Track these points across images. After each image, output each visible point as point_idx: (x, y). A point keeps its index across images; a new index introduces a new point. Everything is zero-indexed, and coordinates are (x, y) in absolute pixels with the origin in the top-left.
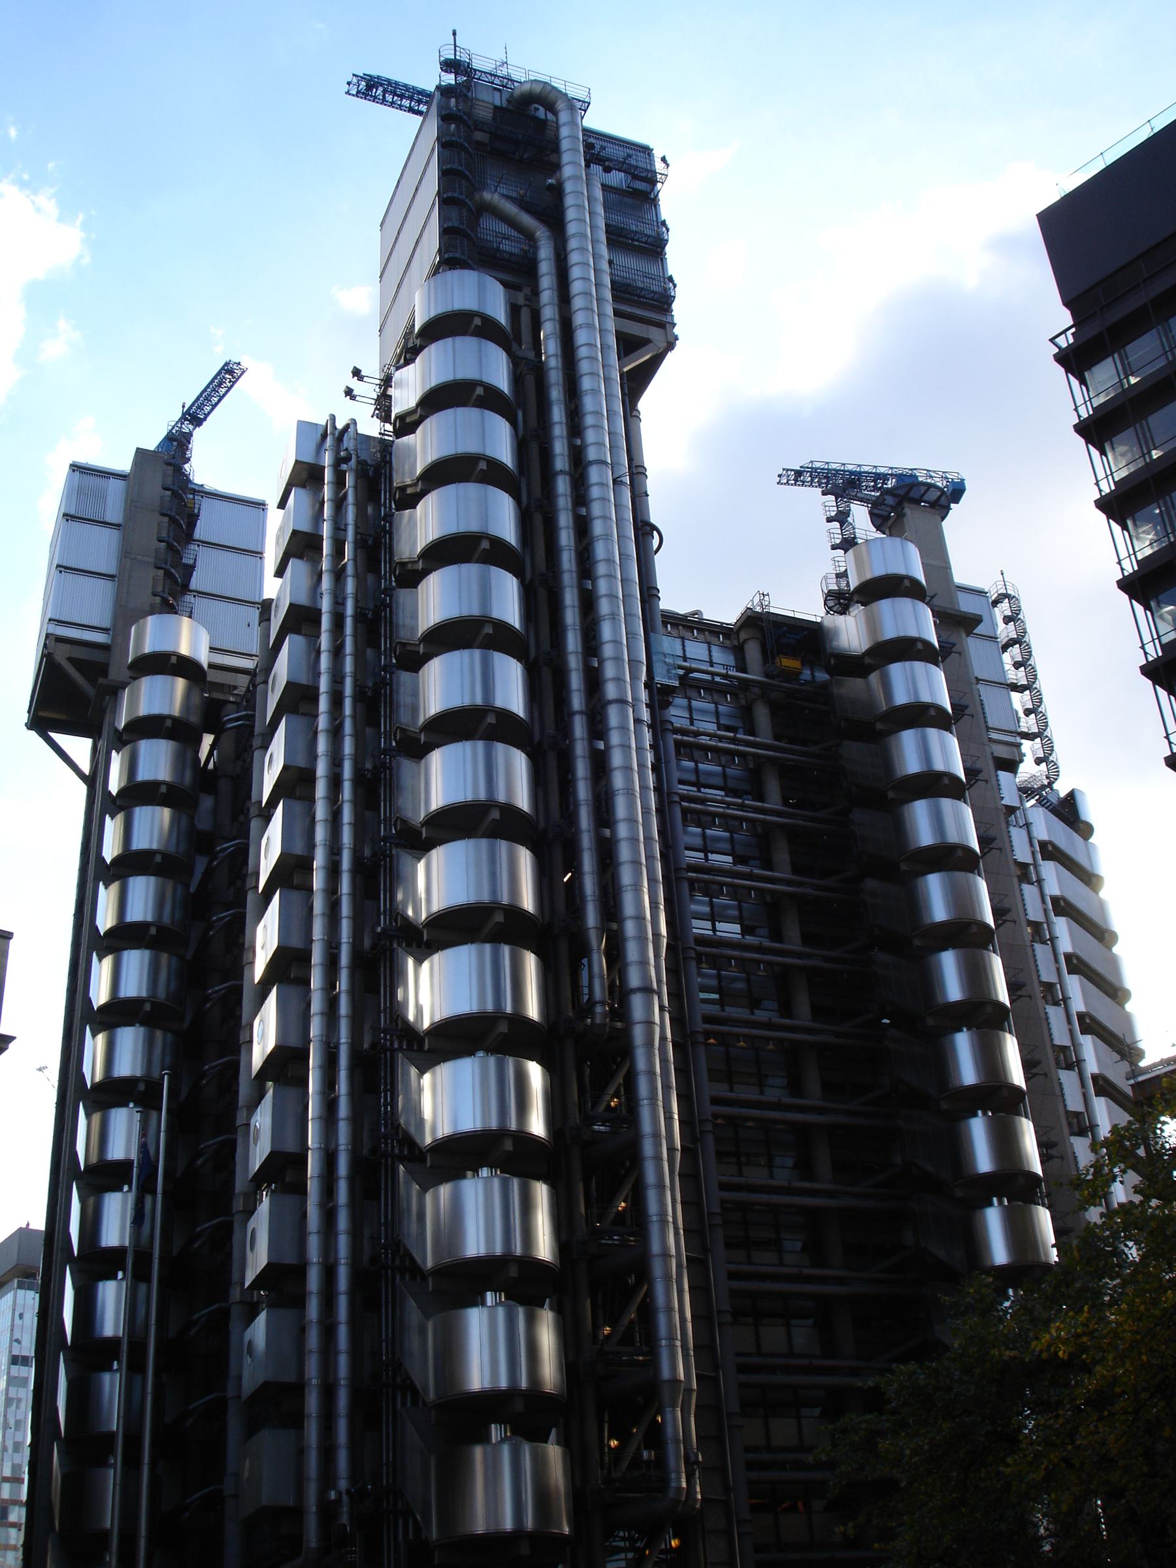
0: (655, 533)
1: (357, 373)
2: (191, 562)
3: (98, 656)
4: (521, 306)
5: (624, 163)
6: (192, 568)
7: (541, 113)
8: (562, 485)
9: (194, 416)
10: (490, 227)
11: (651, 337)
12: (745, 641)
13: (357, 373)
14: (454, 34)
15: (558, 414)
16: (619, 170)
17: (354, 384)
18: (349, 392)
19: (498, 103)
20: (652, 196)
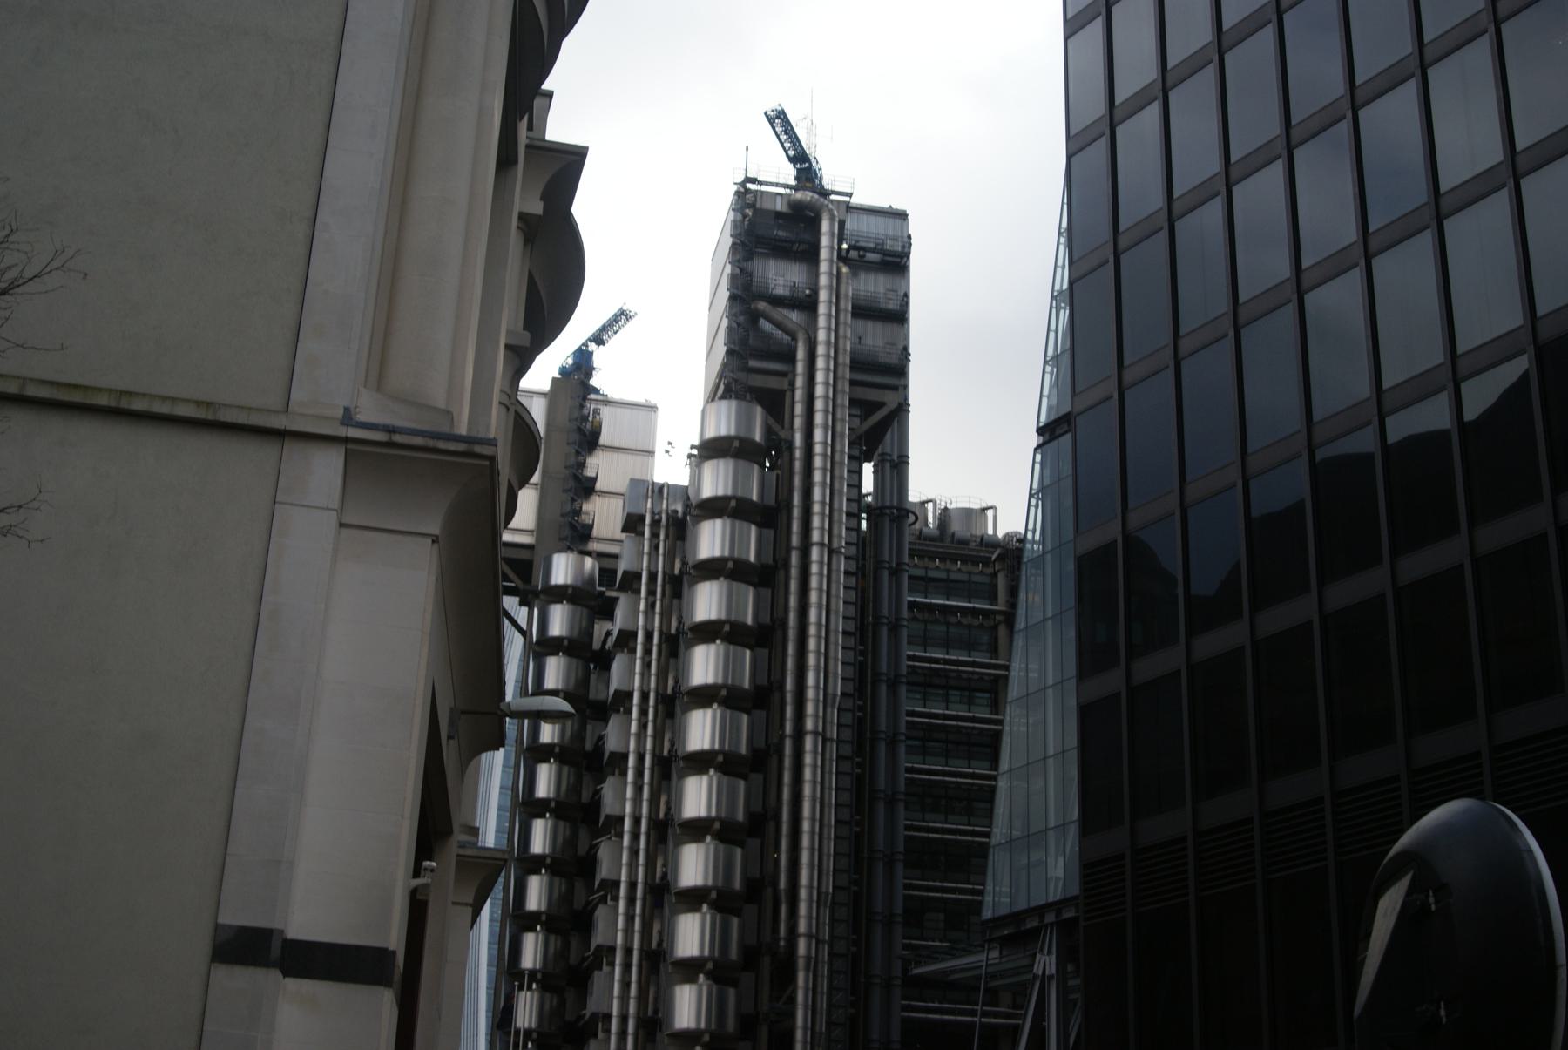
0: (910, 515)
1: (670, 443)
2: (594, 475)
3: (524, 555)
4: (785, 391)
5: (876, 248)
6: (594, 480)
7: (812, 215)
8: (795, 558)
9: (598, 339)
10: (765, 325)
11: (886, 399)
12: (998, 571)
13: (670, 443)
14: (747, 149)
15: (797, 499)
16: (874, 252)
17: (669, 448)
18: (667, 452)
19: (778, 208)
20: (903, 262)
